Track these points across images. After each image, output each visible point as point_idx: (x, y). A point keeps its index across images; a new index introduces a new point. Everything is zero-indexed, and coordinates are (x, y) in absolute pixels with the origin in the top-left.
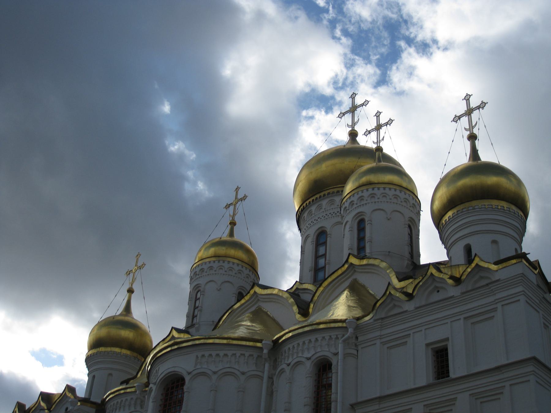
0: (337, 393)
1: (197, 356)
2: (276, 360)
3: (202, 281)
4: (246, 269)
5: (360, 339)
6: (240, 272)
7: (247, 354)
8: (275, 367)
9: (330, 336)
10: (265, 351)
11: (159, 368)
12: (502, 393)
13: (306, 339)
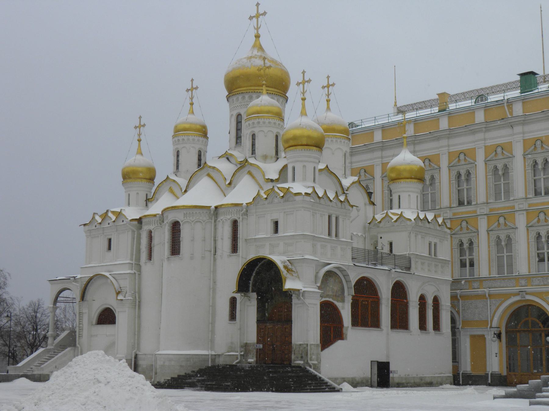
0: (240, 234)
2: (217, 214)
3: (179, 147)
4: (201, 138)
5: (248, 211)
6: (198, 140)
7: (205, 212)
8: (217, 217)
9: (237, 210)
10: (212, 212)
12: (293, 244)
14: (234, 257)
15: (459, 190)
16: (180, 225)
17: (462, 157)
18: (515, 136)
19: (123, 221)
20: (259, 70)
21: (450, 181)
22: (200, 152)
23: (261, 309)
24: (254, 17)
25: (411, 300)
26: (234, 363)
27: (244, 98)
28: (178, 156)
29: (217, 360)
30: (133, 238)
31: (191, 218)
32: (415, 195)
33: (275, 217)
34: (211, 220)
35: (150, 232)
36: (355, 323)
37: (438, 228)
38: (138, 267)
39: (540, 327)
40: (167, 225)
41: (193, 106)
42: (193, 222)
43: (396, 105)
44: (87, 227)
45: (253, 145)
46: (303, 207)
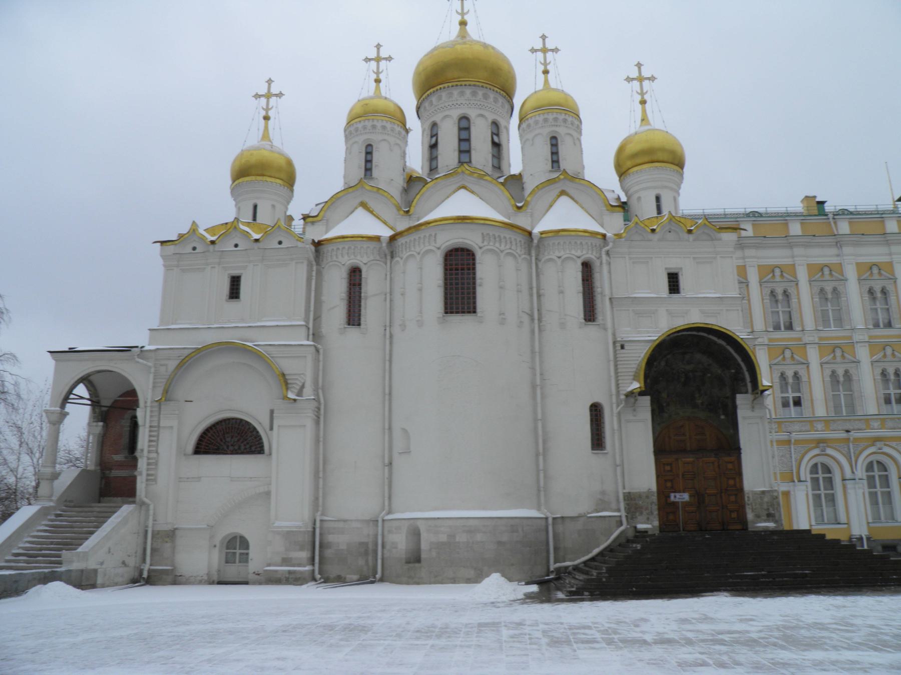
1: (483, 234)
7: (518, 240)
11: (436, 234)
14: (592, 330)
16: (473, 255)
31: (497, 245)
33: (673, 264)
34: (528, 257)
38: (316, 336)
41: (381, 84)
42: (502, 251)
44: (171, 249)
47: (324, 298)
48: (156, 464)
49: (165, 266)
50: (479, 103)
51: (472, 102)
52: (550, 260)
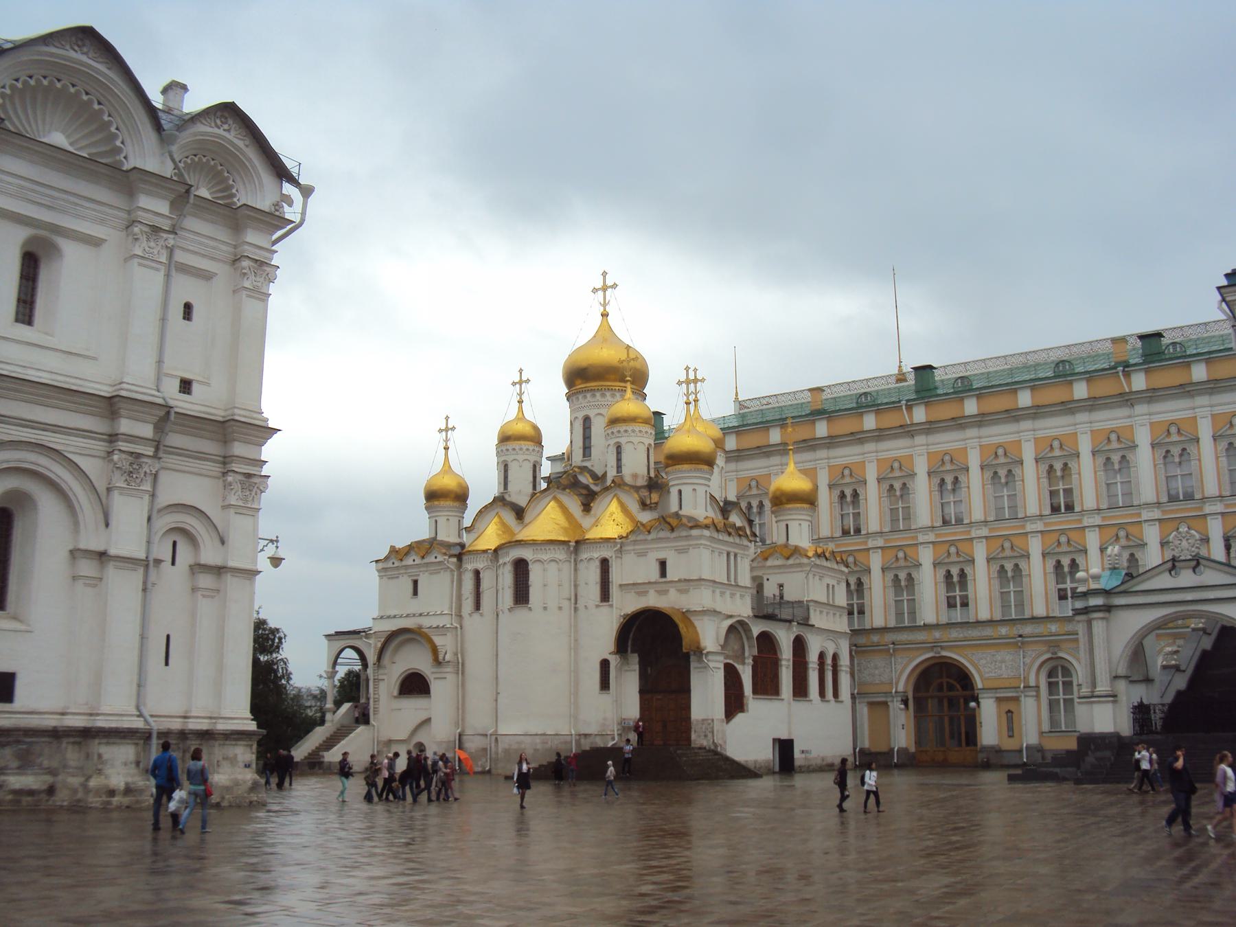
3: (509, 458)
5: (624, 548)
6: (534, 450)
10: (572, 549)
13: (595, 546)
14: (605, 609)
15: (842, 515)
17: (847, 472)
18: (916, 449)
19: (436, 557)
20: (621, 362)
21: (831, 504)
22: (535, 466)
23: (643, 676)
24: (599, 289)
25: (811, 660)
26: (609, 745)
27: (594, 396)
28: (506, 471)
29: (583, 741)
30: (452, 582)
32: (808, 523)
33: (661, 555)
35: (477, 573)
36: (756, 691)
37: (835, 566)
39: (958, 690)
40: (509, 564)
43: (737, 398)
44: (381, 565)
45: (619, 460)
46: (701, 544)
47: (463, 592)
48: (379, 701)
49: (379, 576)
50: (597, 404)
51: (591, 404)
52: (582, 560)
